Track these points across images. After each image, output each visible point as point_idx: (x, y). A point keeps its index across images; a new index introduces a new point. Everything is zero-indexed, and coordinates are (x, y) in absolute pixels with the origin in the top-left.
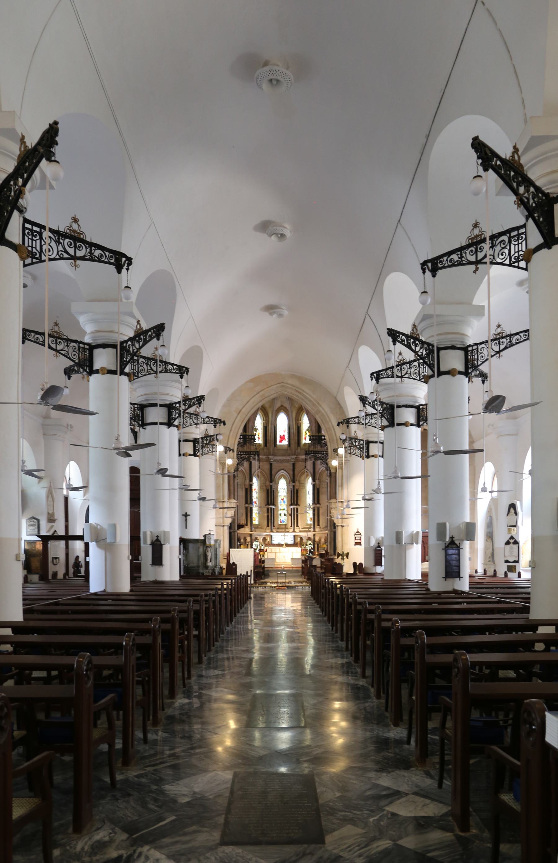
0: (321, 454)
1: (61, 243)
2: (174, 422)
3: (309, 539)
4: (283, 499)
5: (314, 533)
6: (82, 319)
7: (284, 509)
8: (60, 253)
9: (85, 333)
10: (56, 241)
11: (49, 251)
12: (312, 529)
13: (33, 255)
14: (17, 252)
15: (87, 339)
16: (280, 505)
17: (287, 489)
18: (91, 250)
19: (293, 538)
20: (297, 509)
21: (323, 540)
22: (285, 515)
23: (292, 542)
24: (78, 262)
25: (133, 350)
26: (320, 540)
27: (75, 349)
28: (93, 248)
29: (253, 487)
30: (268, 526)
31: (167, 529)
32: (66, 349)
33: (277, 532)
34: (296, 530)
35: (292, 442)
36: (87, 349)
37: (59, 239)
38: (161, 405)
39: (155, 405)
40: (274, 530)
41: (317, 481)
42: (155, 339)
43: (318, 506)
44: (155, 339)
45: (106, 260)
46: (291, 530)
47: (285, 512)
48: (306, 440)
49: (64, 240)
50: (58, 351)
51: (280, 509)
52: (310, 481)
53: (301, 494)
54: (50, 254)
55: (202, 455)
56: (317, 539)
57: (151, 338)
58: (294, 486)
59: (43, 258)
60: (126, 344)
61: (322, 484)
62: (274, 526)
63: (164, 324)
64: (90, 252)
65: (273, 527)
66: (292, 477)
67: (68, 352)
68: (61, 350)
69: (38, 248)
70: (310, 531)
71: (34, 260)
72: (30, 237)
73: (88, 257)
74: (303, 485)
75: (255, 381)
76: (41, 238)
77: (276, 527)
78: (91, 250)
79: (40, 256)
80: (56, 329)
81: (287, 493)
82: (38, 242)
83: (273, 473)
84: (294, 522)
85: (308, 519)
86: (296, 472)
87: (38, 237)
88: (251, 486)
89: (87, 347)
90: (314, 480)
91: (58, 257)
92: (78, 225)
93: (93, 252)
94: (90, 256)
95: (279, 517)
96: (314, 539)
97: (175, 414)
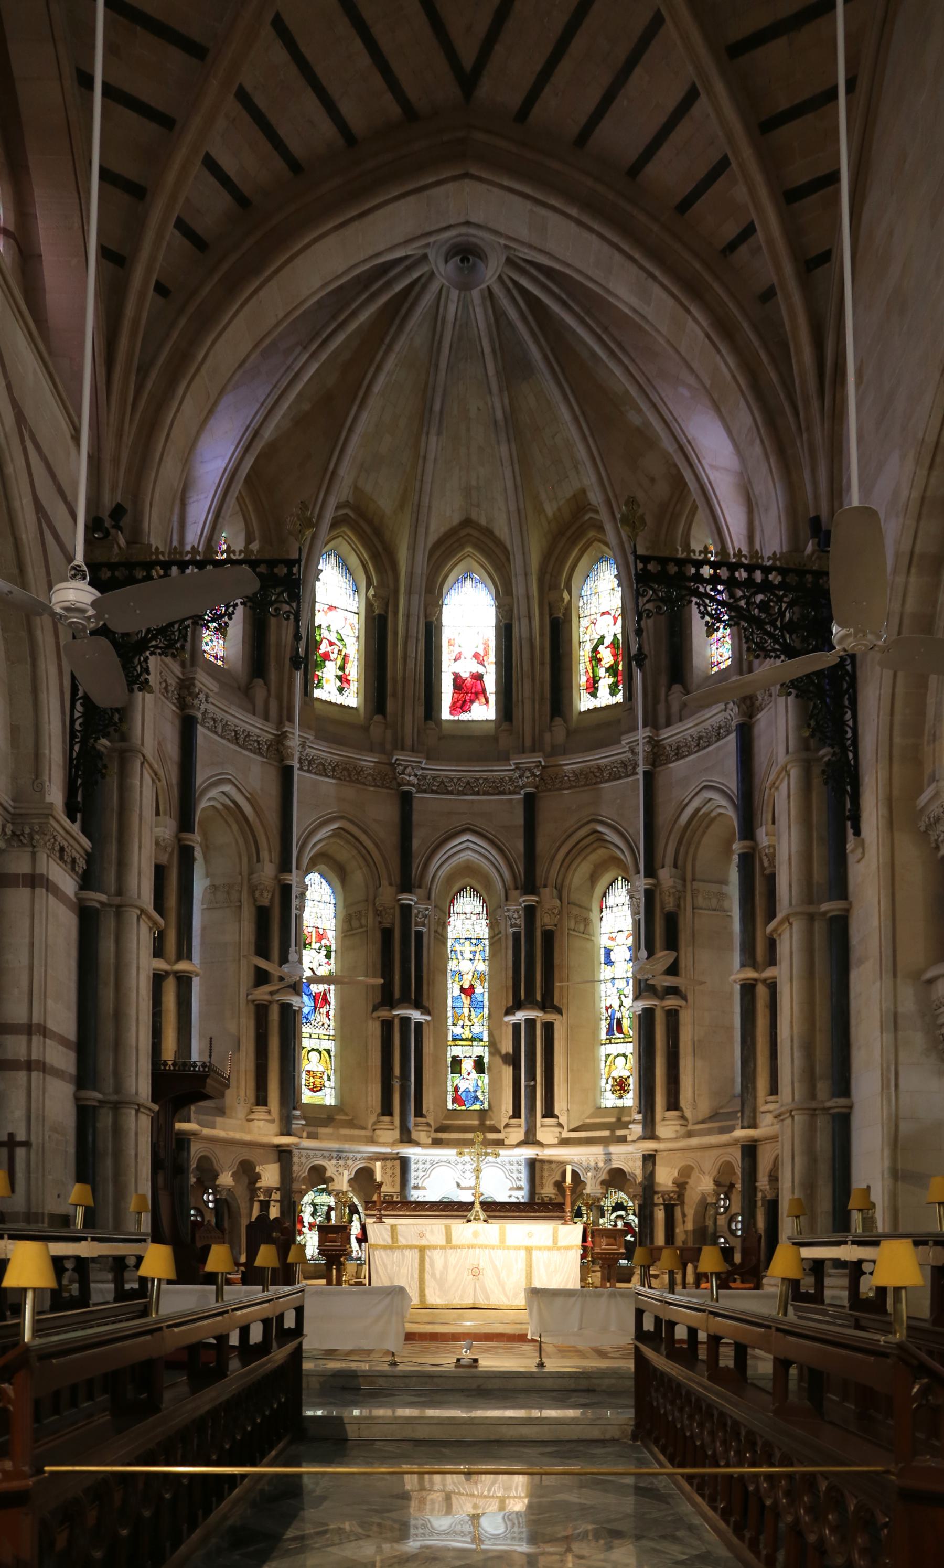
3: (616, 1179)
4: (468, 991)
5: (650, 1145)
12: (637, 1130)
16: (457, 1017)
19: (524, 1175)
20: (549, 1028)
21: (703, 1185)
22: (479, 1066)
23: (521, 1196)
26: (681, 1186)
30: (387, 1110)
33: (437, 1143)
34: (541, 1135)
35: (524, 691)
40: (421, 1135)
41: (666, 875)
46: (517, 1135)
53: (566, 955)
56: (665, 1177)
61: (694, 893)
62: (419, 1113)
65: (412, 1119)
66: (520, 868)
70: (623, 1140)
83: (416, 843)
84: (532, 1091)
95: (450, 1076)
96: (650, 1177)
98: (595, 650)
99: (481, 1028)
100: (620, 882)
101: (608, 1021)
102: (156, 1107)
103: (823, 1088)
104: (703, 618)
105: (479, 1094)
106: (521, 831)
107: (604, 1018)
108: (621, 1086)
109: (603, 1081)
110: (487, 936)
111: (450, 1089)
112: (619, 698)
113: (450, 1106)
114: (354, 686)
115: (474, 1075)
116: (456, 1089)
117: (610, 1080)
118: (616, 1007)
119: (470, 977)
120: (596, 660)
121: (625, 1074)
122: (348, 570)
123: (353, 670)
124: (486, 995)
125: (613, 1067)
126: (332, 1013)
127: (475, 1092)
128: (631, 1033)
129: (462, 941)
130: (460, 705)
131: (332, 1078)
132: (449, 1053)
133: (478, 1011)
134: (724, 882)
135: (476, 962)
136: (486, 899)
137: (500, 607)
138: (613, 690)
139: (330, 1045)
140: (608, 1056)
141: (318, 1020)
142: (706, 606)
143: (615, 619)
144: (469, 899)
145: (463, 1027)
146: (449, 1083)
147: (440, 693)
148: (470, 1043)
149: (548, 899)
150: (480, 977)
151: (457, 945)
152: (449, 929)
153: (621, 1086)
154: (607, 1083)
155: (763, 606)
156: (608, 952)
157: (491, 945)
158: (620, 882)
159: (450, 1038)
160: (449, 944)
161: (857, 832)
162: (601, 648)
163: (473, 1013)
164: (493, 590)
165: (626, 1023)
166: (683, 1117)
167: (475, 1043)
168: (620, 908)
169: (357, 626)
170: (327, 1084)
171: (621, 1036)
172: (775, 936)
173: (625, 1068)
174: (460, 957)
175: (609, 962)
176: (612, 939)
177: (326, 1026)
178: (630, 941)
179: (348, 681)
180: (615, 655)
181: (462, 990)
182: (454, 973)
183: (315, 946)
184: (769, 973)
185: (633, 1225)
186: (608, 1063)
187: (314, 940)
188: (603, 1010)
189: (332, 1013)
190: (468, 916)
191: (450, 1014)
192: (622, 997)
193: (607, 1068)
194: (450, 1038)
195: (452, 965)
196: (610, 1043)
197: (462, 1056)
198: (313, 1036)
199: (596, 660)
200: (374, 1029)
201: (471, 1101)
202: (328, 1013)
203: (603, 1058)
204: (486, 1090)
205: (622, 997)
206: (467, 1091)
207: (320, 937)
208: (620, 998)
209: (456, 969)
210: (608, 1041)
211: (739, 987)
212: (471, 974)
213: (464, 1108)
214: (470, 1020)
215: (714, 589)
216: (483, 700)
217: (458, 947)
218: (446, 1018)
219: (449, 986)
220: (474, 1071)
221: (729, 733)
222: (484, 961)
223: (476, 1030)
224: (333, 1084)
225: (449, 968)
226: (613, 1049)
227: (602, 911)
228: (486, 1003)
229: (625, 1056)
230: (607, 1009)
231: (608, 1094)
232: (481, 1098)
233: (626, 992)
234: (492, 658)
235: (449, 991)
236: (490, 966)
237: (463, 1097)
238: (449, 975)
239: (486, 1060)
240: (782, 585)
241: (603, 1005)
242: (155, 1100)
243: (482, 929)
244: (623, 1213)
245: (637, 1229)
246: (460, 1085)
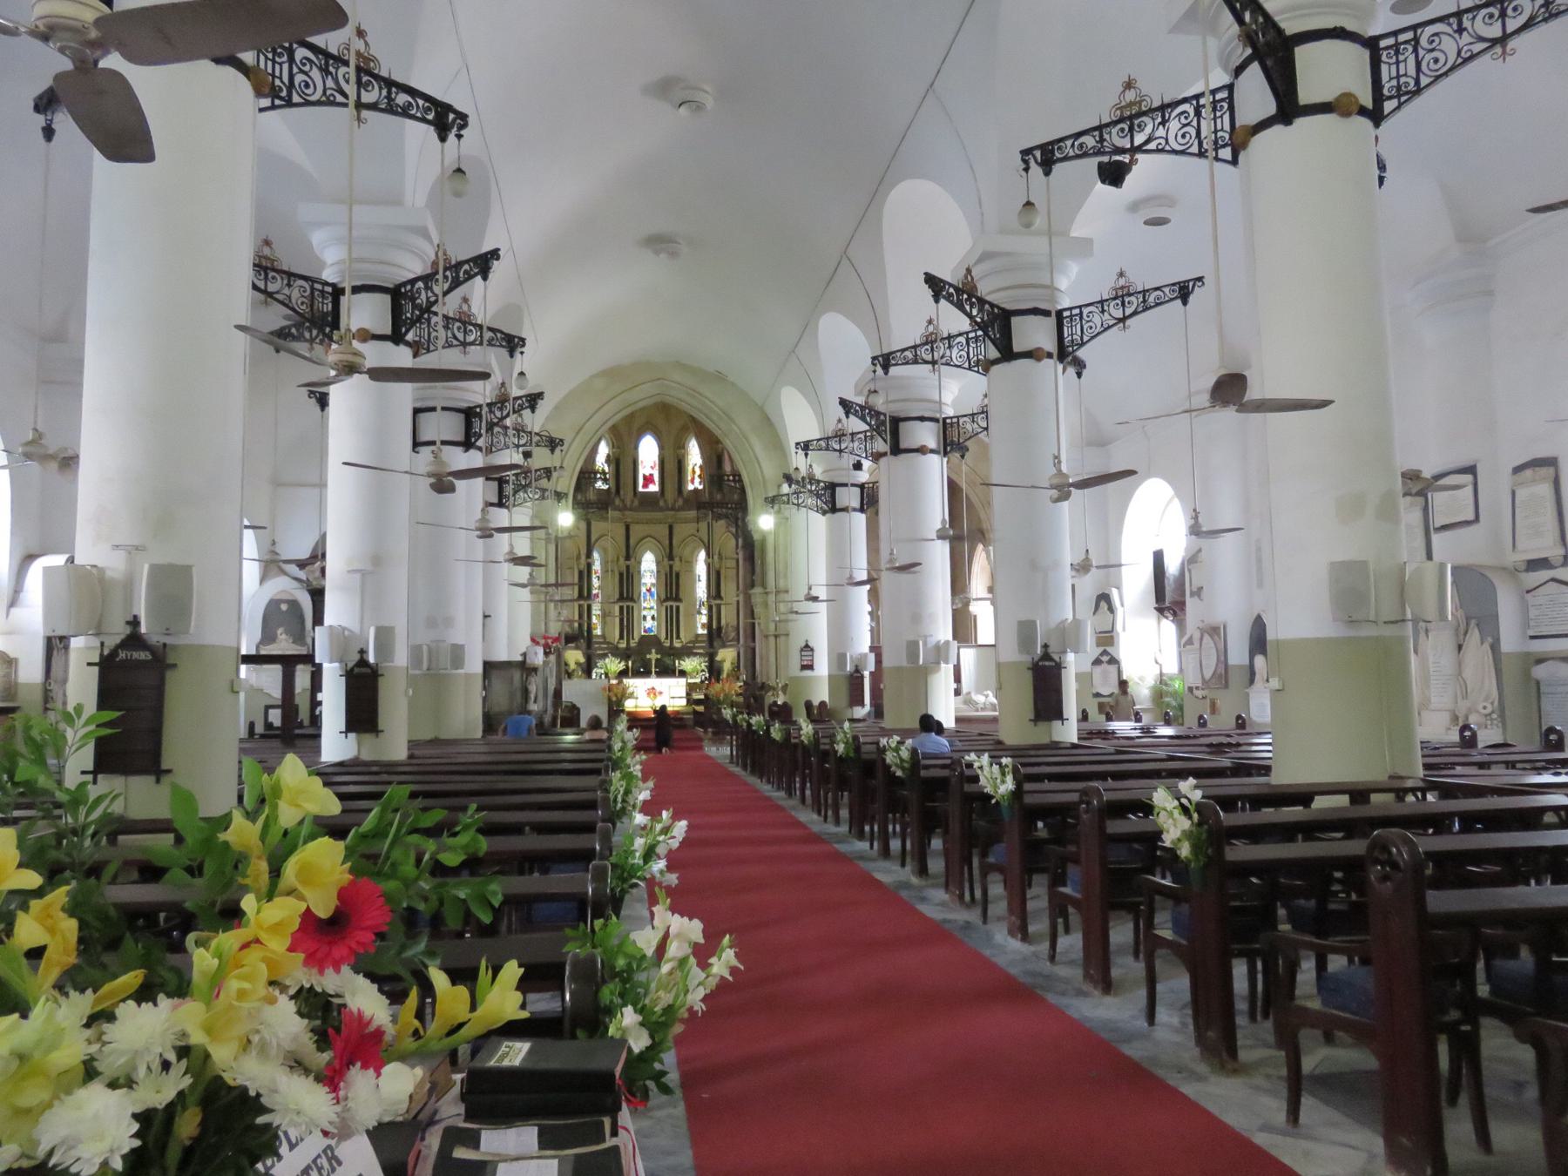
0: (727, 508)
1: (331, 73)
2: (476, 441)
4: (649, 590)
6: (317, 238)
7: (652, 608)
8: (329, 92)
9: (322, 265)
10: (320, 69)
11: (307, 86)
13: (274, 93)
14: (248, 78)
15: (329, 275)
16: (645, 601)
17: (658, 572)
18: (389, 92)
20: (678, 608)
22: (653, 618)
24: (365, 113)
25: (428, 298)
27: (304, 291)
28: (394, 89)
29: (594, 568)
31: (460, 641)
32: (286, 291)
36: (328, 293)
37: (327, 64)
38: (444, 409)
39: (433, 409)
42: (479, 279)
43: (718, 602)
44: (479, 279)
45: (419, 115)
47: (653, 612)
48: (694, 484)
49: (337, 69)
50: (270, 295)
51: (645, 608)
52: (702, 555)
54: (309, 91)
55: (514, 505)
57: (470, 277)
58: (671, 567)
59: (296, 99)
60: (413, 286)
63: (499, 249)
64: (388, 97)
66: (668, 550)
67: (290, 297)
68: (277, 292)
69: (286, 79)
71: (277, 102)
72: (270, 56)
73: (383, 106)
74: (690, 564)
75: (611, 374)
76: (291, 60)
78: (389, 92)
79: (290, 94)
80: (267, 251)
81: (658, 578)
82: (286, 67)
84: (672, 631)
85: (699, 626)
86: (675, 542)
87: (285, 58)
88: (589, 566)
89: (329, 289)
90: (708, 554)
91: (324, 99)
92: (367, 44)
93: (393, 96)
94: (388, 104)
97: (480, 426)
99: (653, 604)
115: (651, 622)
122: (608, 444)
150: (653, 585)
173: (704, 619)
195: (643, 581)
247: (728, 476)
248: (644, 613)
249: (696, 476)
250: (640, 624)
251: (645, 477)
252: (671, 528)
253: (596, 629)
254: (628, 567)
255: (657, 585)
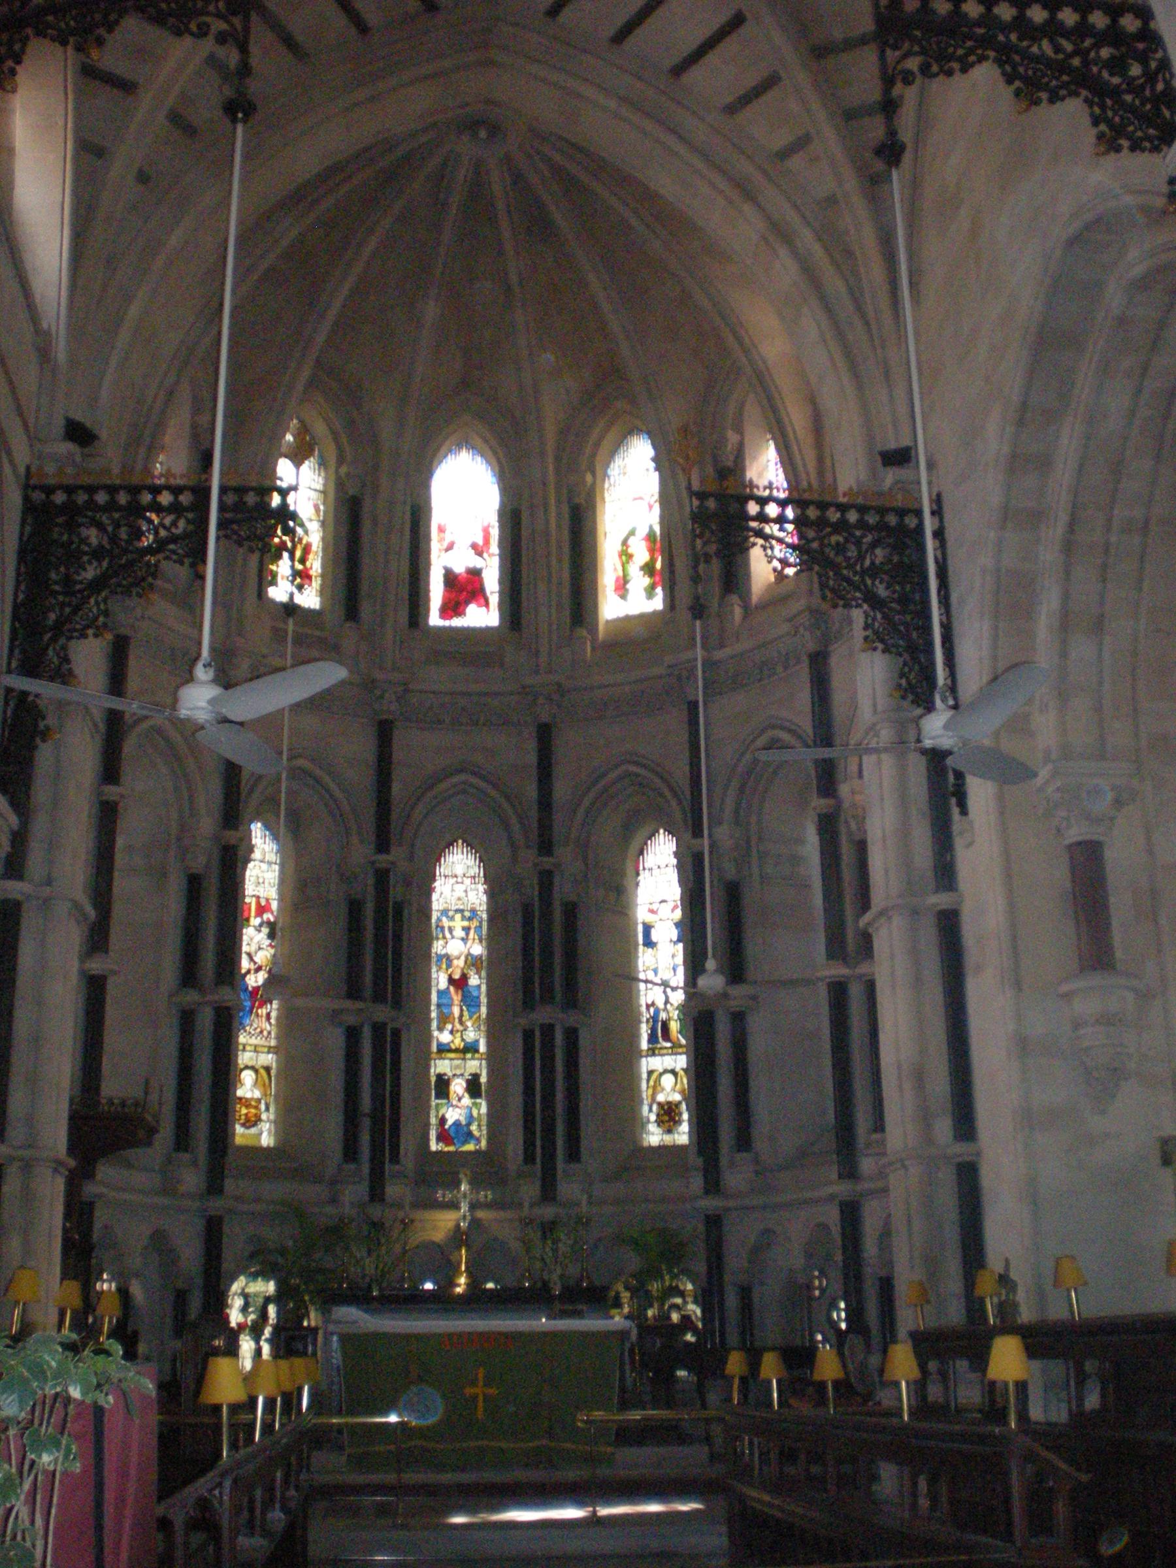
4: (460, 983)
7: (470, 1049)
16: (444, 1019)
22: (473, 1087)
51: (443, 1049)
77: (408, 1162)
95: (434, 1102)
98: (625, 543)
100: (662, 836)
101: (651, 1023)
102: (72, 1163)
103: (944, 1127)
104: (770, 562)
105: (474, 1128)
106: (534, 772)
107: (644, 1019)
108: (668, 1116)
109: (645, 1109)
110: (484, 907)
111: (433, 1121)
112: (657, 603)
113: (434, 1146)
114: (316, 583)
115: (467, 1101)
116: (443, 1120)
117: (655, 1107)
118: (661, 1005)
119: (460, 963)
120: (626, 555)
121: (677, 1097)
123: (315, 565)
124: (484, 988)
125: (659, 1088)
126: (274, 1014)
127: (469, 1124)
128: (683, 1041)
129: (451, 913)
130: (452, 608)
131: (272, 1109)
132: (432, 1070)
133: (473, 1010)
134: (800, 841)
135: (470, 943)
136: (485, 858)
137: (505, 490)
138: (650, 592)
139: (268, 1059)
140: (650, 1073)
141: (255, 1025)
142: (772, 548)
143: (651, 507)
144: (460, 856)
145: (452, 1032)
146: (433, 1113)
147: (428, 591)
148: (461, 1056)
149: (564, 854)
150: (474, 962)
151: (444, 919)
152: (435, 896)
153: (668, 1116)
154: (650, 1110)
155: (840, 549)
156: (648, 928)
157: (492, 919)
158: (662, 836)
159: (434, 1048)
160: (434, 920)
161: (964, 812)
162: (631, 541)
163: (466, 1013)
164: (497, 469)
165: (674, 1026)
166: (756, 1161)
167: (469, 1056)
168: (663, 870)
169: (322, 507)
170: (264, 1116)
171: (668, 1045)
172: (870, 930)
174: (448, 935)
175: (649, 943)
176: (652, 911)
177: (265, 1033)
178: (678, 914)
179: (309, 577)
180: (652, 551)
181: (451, 981)
182: (440, 958)
183: (256, 921)
184: (863, 969)
185: (693, 1318)
186: (652, 1083)
187: (253, 913)
188: (643, 1009)
189: (274, 1014)
190: (460, 880)
191: (434, 1015)
192: (668, 990)
193: (650, 1091)
194: (434, 1048)
195: (438, 947)
196: (654, 1054)
197: (450, 1074)
198: (248, 1048)
199: (626, 555)
200: (335, 1040)
201: (462, 1139)
202: (268, 1016)
203: (645, 1076)
204: (484, 1122)
205: (668, 990)
206: (457, 1124)
207: (261, 910)
208: (665, 992)
209: (443, 952)
210: (650, 1053)
211: (825, 987)
212: (463, 958)
213: (451, 1148)
214: (461, 1022)
215: (781, 529)
216: (482, 601)
217: (446, 922)
218: (429, 1020)
219: (434, 975)
220: (466, 1095)
221: (798, 662)
222: (481, 941)
223: (471, 1035)
224: (272, 1117)
225: (434, 950)
226: (656, 1063)
227: (638, 874)
228: (484, 1000)
229: (673, 1072)
230: (648, 1006)
231: (652, 1127)
232: (476, 1133)
233: (673, 983)
234: (494, 548)
235: (434, 983)
236: (490, 949)
237: (452, 1133)
238: (434, 960)
239: (483, 1079)
240: (862, 524)
241: (643, 1002)
242: (71, 1150)
243: (477, 897)
244: (678, 1301)
245: (700, 1325)
246: (447, 1116)
247: (763, 502)
248: (442, 1066)
249: (634, 570)
250: (423, 1109)
251: (450, 579)
252: (545, 735)
253: (252, 1122)
254: (382, 877)
255: (492, 964)
